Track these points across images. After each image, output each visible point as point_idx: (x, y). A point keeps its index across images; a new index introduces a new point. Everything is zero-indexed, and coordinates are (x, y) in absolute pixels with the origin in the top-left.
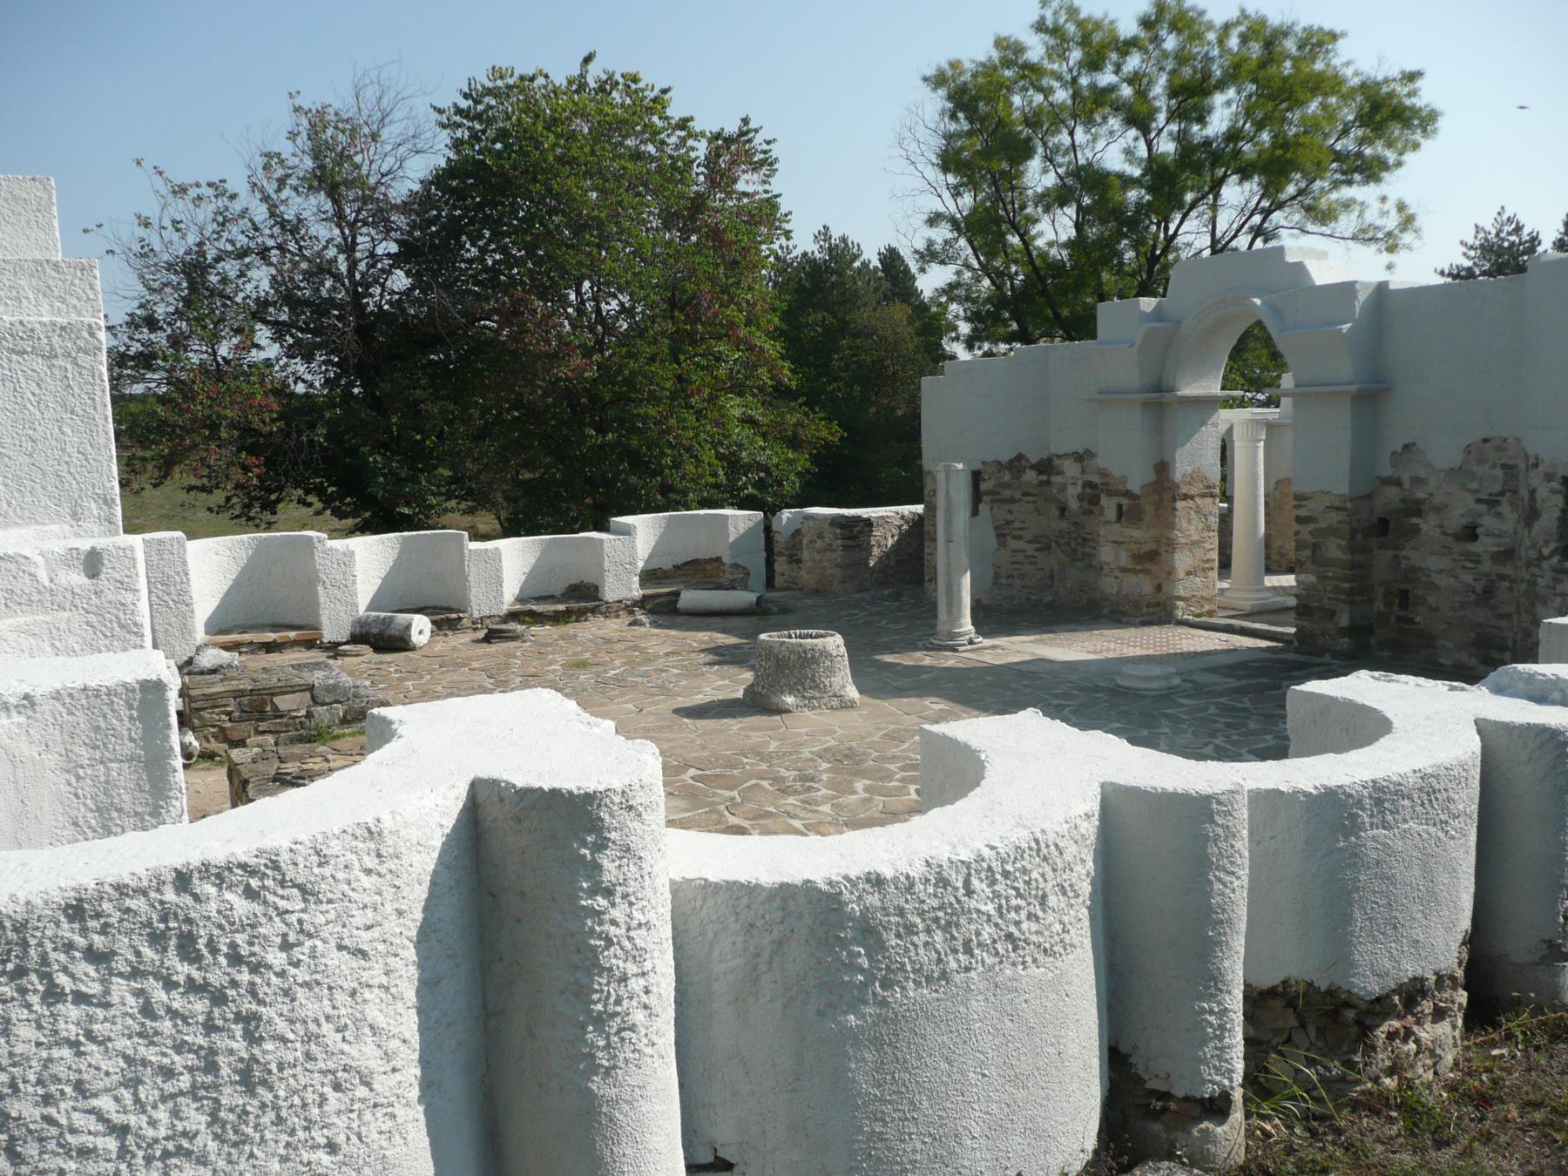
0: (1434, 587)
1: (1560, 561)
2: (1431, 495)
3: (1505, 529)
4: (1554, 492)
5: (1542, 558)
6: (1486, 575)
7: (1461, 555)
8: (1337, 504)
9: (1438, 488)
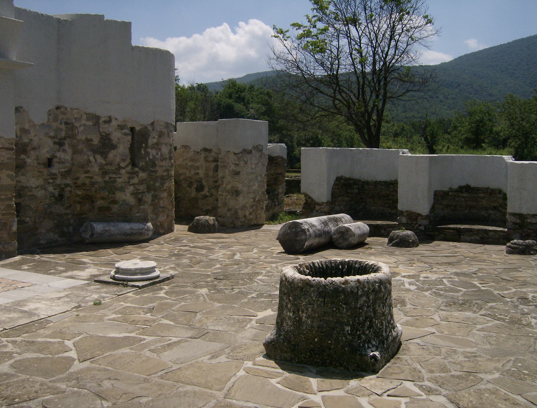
0: (34, 197)
1: (132, 169)
2: (31, 140)
3: (67, 158)
4: (126, 134)
5: (120, 168)
6: (59, 186)
7: (48, 175)
8: (7, 145)
9: (35, 136)
